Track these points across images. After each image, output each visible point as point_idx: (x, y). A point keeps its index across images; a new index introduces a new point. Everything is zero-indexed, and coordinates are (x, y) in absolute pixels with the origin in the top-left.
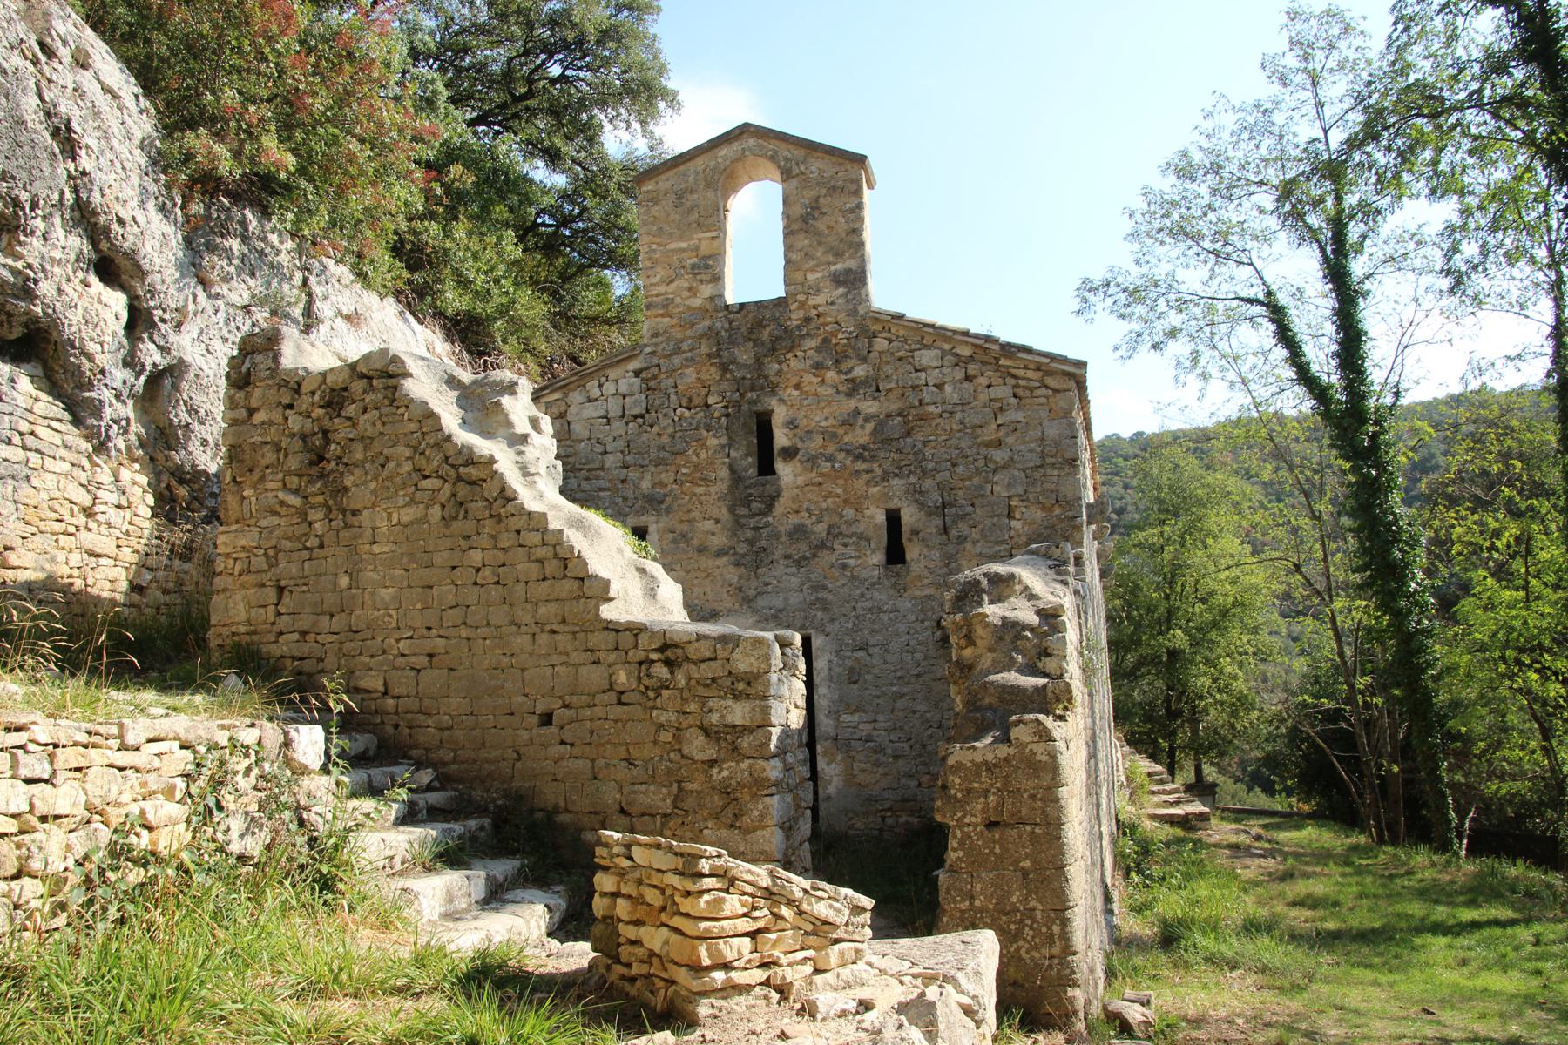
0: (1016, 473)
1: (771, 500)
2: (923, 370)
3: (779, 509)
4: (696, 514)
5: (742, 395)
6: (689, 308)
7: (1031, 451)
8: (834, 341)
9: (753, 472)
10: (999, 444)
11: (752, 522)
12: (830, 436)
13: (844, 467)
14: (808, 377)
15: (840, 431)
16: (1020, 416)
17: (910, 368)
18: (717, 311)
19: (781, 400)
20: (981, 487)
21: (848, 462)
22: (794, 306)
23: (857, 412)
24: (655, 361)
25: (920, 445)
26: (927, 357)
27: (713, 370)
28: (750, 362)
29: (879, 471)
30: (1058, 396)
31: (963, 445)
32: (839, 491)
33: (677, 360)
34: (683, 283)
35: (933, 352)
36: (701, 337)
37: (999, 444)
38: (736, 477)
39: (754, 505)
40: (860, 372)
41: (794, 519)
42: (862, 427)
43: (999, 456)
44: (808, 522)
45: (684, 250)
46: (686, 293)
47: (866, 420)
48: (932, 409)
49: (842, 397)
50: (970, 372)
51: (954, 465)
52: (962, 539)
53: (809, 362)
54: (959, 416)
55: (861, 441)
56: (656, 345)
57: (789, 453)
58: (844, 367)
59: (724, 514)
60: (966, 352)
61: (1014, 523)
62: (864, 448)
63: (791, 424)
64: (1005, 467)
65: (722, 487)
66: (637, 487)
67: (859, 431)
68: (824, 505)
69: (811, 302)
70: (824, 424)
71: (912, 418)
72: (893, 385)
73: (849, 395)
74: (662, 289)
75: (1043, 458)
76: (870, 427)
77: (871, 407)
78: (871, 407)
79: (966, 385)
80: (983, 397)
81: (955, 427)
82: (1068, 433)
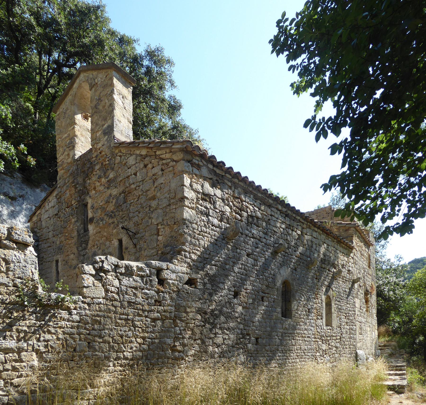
0: (160, 211)
1: (87, 242)
2: (130, 168)
3: (89, 246)
4: (69, 252)
5: (80, 197)
6: (68, 163)
7: (165, 198)
8: (104, 164)
9: (82, 231)
10: (154, 198)
11: (82, 253)
12: (103, 209)
13: (106, 223)
14: (98, 184)
15: (106, 206)
16: (161, 180)
17: (126, 168)
18: (74, 162)
19: (90, 197)
20: (148, 222)
21: (107, 220)
22: (93, 152)
23: (111, 195)
24: (60, 190)
25: (128, 206)
26: (131, 160)
27: (73, 189)
28: (82, 182)
29: (116, 222)
30: (178, 164)
31: (142, 202)
32: (105, 234)
33: (65, 188)
34: (66, 153)
35: (134, 157)
36: (70, 175)
37: (154, 198)
38: (79, 235)
39: (84, 245)
40: (111, 176)
41: (93, 250)
42: (112, 202)
43: (154, 204)
44: (97, 250)
45: (66, 138)
46: (67, 157)
47: (113, 199)
48: (133, 186)
49: (106, 190)
50: (146, 163)
51: (139, 213)
52: (141, 249)
53: (97, 176)
54: (141, 187)
55: (112, 209)
56: (60, 183)
57: (92, 220)
58: (107, 174)
59: (75, 251)
60: (144, 152)
61: (160, 238)
62: (112, 212)
63: (93, 207)
64: (156, 209)
65: (76, 239)
66: (56, 243)
67: (111, 205)
68: (101, 242)
69: (98, 147)
70: (101, 204)
71: (126, 193)
72: (121, 179)
73: (108, 188)
74: (61, 158)
75: (169, 201)
76: (114, 201)
77: (115, 192)
78: (115, 192)
79: (144, 170)
80: (150, 174)
81: (140, 193)
82: (180, 184)
